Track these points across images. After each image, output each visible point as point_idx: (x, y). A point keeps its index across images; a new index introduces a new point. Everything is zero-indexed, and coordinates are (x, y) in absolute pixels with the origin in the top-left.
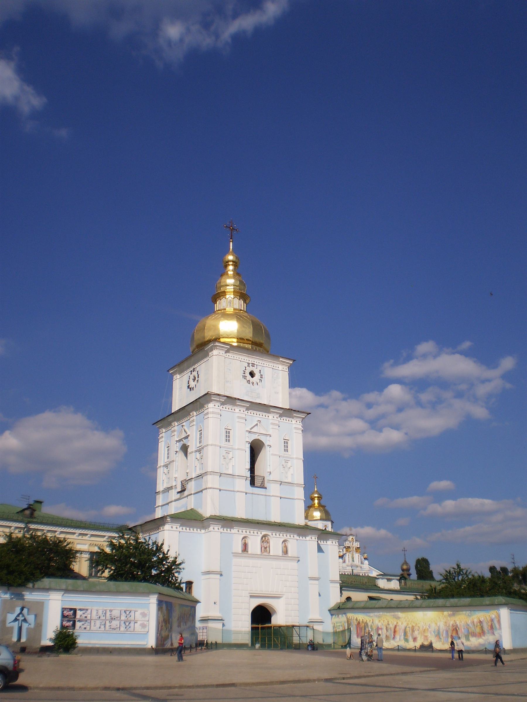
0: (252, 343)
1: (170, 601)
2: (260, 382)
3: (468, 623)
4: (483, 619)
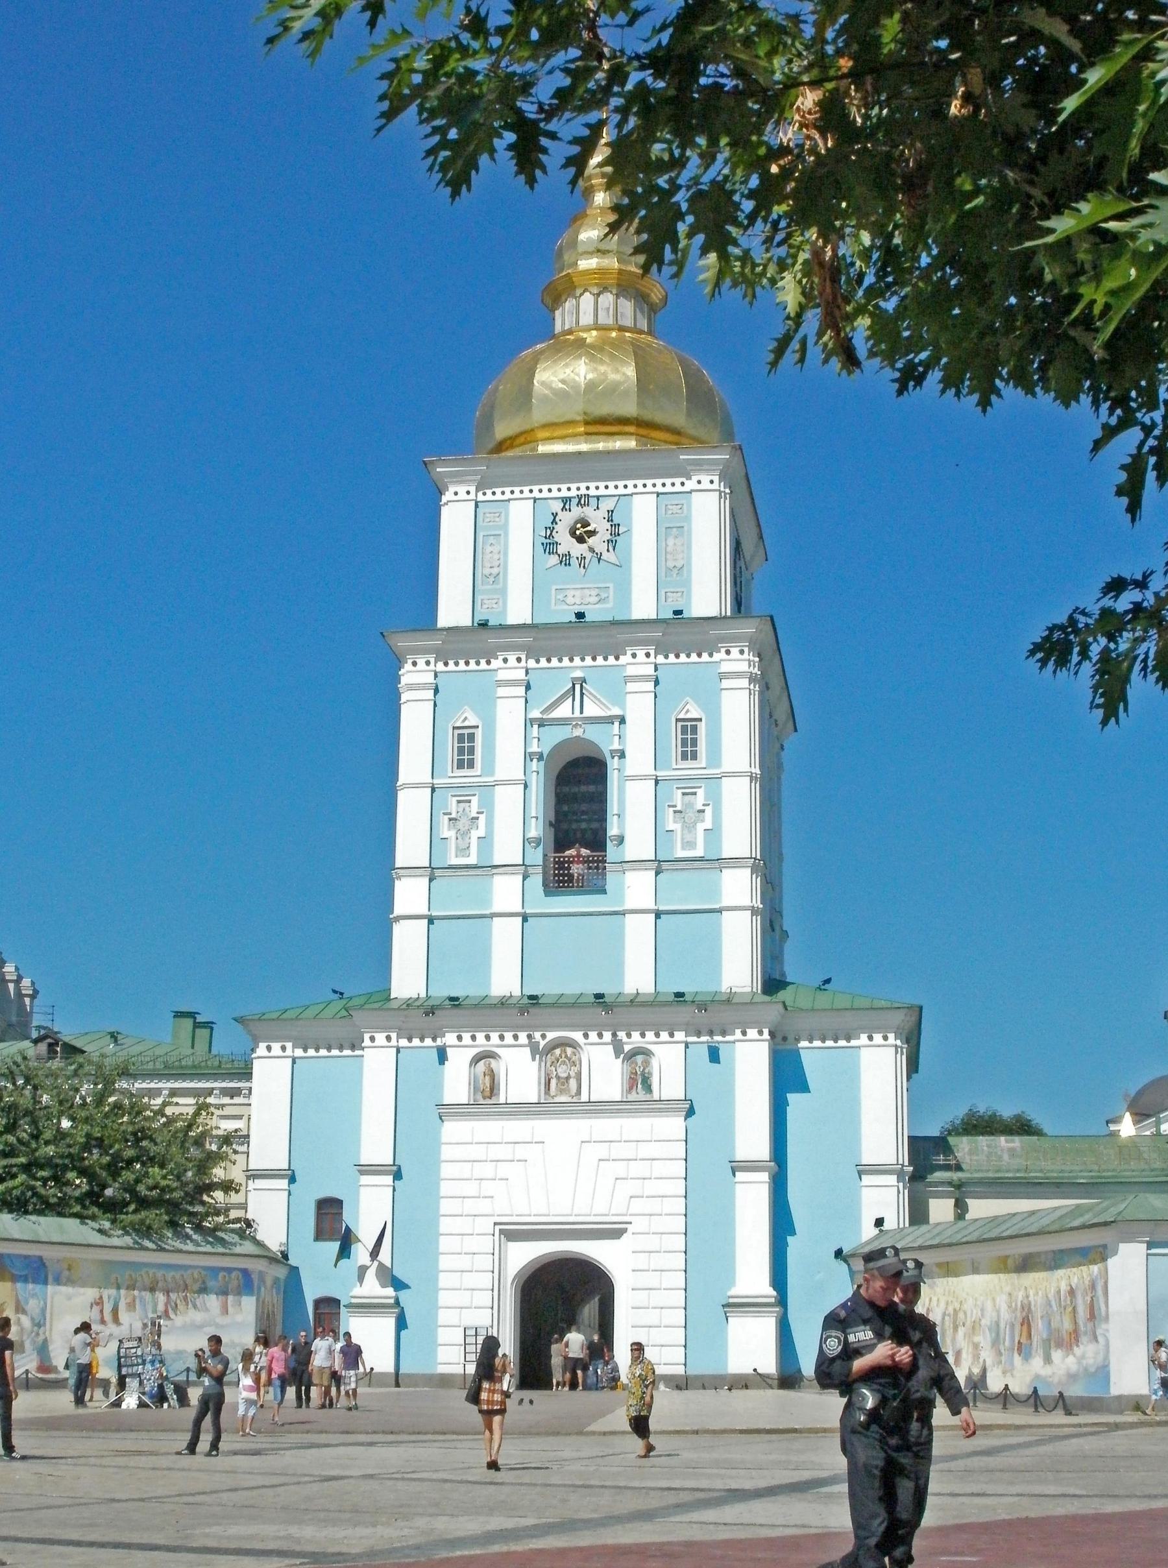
0: (592, 429)
1: (37, 1253)
2: (608, 550)
3: (1049, 1296)
4: (1076, 1280)
